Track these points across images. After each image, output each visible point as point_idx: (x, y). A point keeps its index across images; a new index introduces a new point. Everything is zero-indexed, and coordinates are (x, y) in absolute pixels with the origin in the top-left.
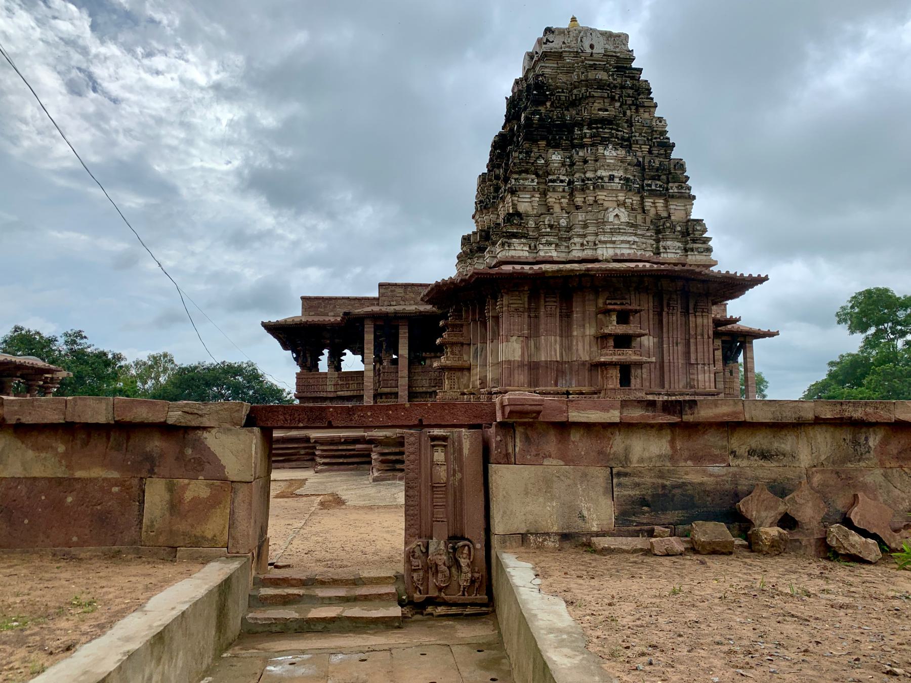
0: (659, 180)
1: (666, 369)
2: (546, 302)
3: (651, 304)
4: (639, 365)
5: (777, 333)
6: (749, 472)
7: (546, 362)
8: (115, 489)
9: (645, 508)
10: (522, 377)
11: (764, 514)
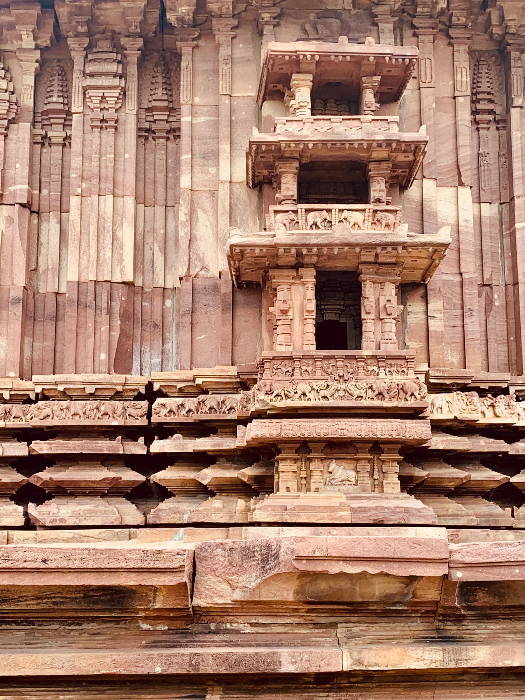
3: (464, 78)
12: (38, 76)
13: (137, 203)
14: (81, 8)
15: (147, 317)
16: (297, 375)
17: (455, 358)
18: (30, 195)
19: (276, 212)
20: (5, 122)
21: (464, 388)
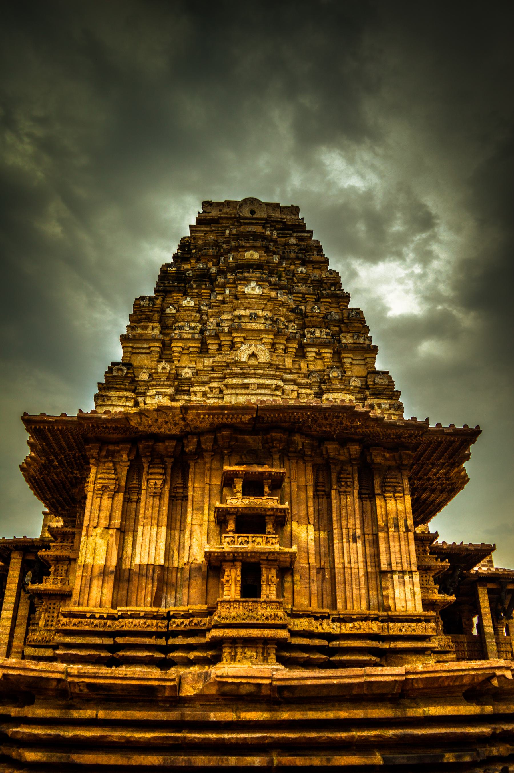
1: (339, 578)
3: (311, 477)
12: (128, 471)
13: (167, 528)
14: (148, 445)
15: (169, 581)
16: (232, 609)
17: (306, 602)
18: (121, 523)
19: (225, 537)
20: (113, 493)
21: (308, 616)
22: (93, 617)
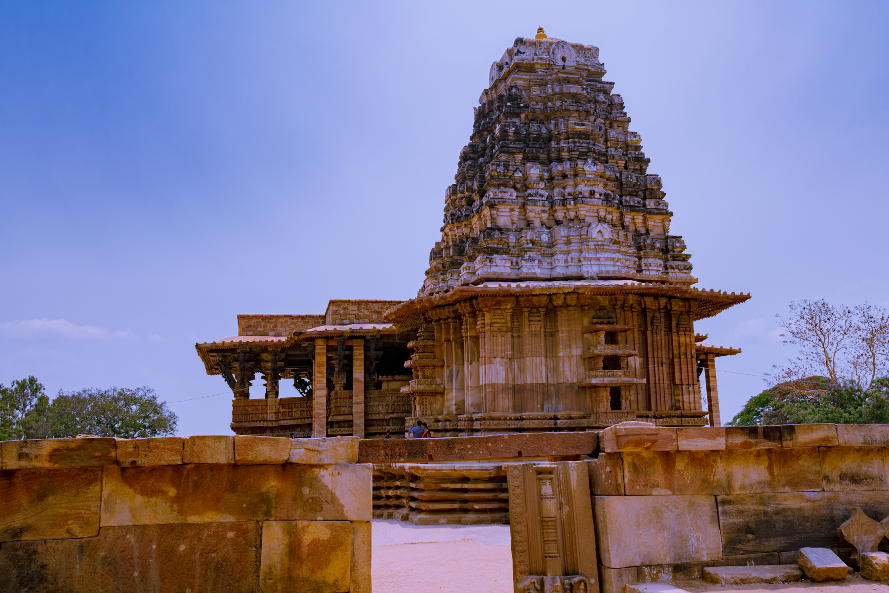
0: (636, 196)
1: (652, 390)
2: (530, 321)
4: (629, 386)
5: (739, 351)
6: (843, 497)
7: (532, 384)
8: (230, 535)
9: (750, 536)
10: (506, 401)
11: (865, 538)
22: (505, 419)
